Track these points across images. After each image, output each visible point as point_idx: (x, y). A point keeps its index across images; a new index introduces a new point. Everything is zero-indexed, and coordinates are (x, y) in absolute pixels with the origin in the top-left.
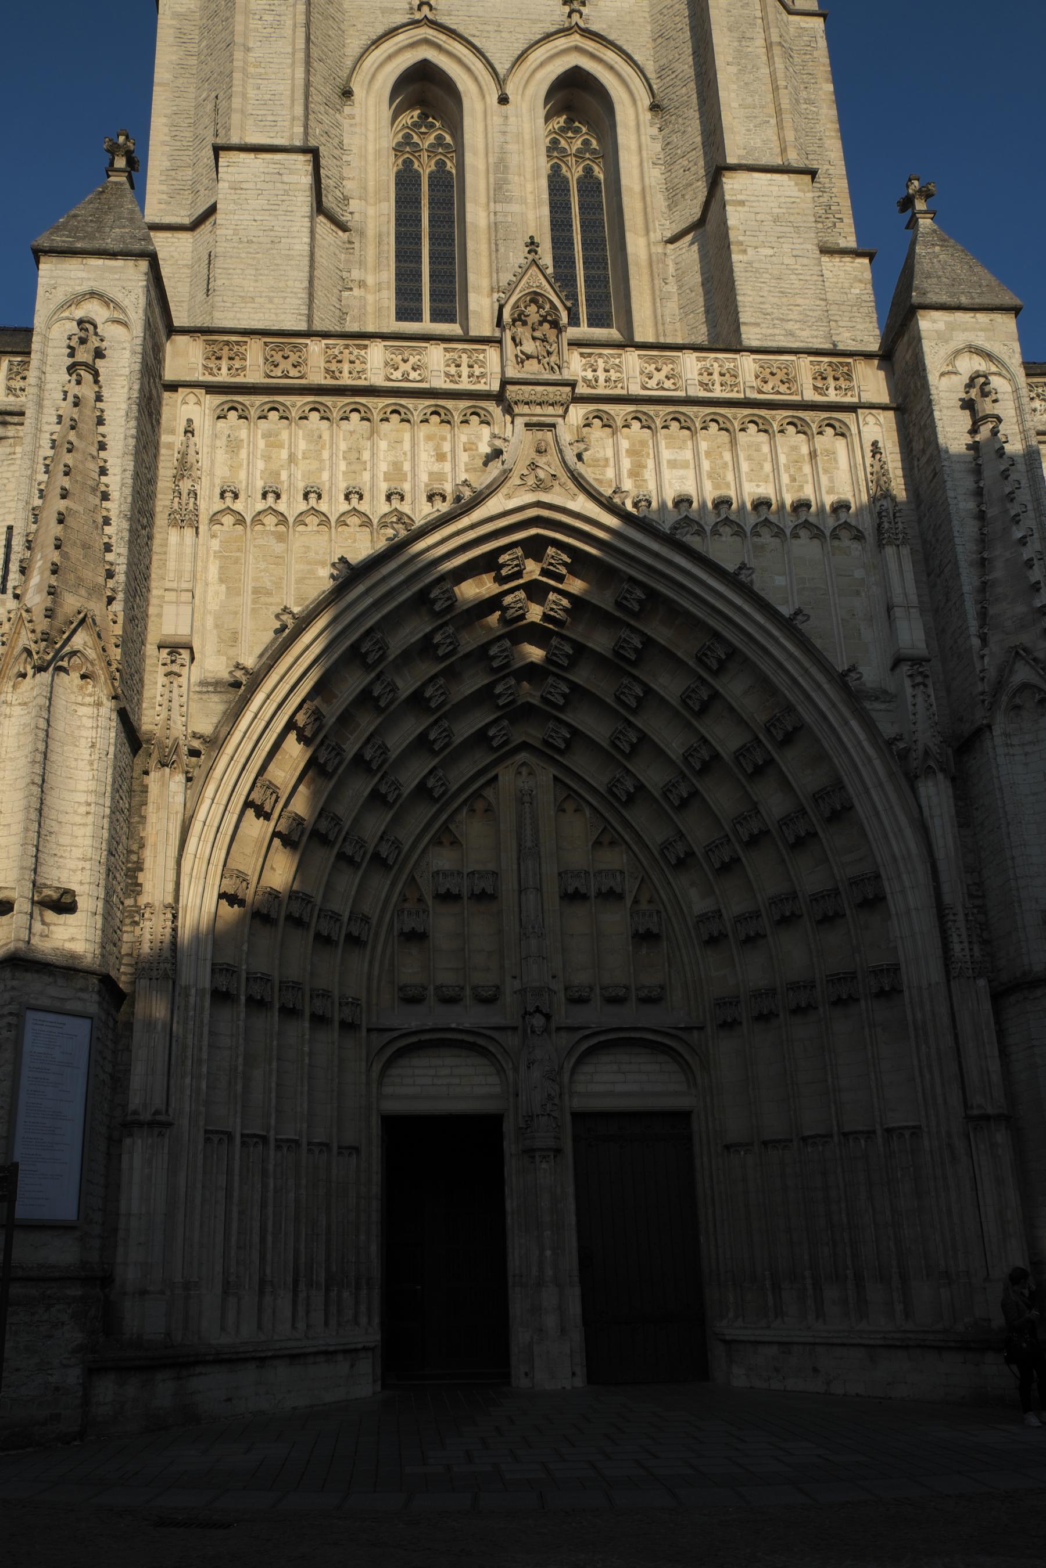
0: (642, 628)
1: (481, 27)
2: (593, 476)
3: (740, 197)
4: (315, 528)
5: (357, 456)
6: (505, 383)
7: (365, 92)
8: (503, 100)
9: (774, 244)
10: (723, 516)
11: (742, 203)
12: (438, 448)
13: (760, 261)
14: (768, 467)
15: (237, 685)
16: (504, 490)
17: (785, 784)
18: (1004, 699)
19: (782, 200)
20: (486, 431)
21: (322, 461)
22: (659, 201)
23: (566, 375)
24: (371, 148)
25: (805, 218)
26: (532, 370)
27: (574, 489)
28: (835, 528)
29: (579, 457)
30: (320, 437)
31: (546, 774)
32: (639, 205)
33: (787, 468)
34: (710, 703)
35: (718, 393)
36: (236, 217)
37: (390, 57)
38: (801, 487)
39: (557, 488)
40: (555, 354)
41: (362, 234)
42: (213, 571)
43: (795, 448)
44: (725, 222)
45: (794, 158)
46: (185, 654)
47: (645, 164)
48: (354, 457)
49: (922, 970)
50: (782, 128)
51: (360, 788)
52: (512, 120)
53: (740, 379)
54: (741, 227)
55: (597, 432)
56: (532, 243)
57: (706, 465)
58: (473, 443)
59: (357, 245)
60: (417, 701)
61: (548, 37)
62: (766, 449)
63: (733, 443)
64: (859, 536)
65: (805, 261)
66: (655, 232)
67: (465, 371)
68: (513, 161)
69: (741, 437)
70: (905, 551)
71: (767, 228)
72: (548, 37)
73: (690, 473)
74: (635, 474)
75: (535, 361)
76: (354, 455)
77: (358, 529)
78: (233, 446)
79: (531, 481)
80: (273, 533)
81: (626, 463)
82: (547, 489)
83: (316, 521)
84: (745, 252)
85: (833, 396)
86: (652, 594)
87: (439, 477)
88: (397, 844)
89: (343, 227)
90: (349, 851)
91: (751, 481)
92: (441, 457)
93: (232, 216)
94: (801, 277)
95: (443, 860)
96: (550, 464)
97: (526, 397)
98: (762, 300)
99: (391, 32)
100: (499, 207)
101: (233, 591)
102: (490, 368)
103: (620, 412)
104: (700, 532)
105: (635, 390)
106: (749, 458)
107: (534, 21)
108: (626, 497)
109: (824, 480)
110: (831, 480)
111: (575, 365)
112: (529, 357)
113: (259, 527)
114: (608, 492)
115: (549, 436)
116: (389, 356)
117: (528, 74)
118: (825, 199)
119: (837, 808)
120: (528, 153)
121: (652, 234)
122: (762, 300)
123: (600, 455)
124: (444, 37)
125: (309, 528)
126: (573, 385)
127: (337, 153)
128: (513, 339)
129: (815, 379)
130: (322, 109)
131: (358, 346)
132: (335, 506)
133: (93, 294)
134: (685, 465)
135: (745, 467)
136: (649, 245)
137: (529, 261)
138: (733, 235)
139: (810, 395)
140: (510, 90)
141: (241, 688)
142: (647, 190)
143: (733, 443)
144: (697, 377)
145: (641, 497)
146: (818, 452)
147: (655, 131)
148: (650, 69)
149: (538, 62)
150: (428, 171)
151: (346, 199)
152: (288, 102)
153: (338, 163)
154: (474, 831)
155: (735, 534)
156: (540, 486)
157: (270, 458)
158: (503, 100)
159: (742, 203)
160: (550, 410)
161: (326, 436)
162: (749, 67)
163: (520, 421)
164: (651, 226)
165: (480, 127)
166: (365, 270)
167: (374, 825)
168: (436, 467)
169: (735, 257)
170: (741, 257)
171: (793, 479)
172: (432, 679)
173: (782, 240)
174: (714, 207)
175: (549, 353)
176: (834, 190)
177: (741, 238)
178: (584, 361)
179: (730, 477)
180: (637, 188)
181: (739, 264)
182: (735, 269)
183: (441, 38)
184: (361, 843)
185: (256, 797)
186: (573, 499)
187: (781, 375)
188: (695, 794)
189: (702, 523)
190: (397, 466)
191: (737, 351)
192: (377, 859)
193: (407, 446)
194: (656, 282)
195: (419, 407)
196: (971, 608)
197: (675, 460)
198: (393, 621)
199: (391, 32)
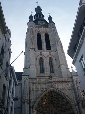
17: (68, 106)
31: (52, 105)
34: (63, 101)
72: (49, 55)
74: (57, 86)
85: (68, 81)
95: (46, 112)
99: (39, 55)
119: (71, 108)
133: (26, 78)
140: (47, 59)
141: (35, 102)
188: (62, 107)
199: (39, 55)
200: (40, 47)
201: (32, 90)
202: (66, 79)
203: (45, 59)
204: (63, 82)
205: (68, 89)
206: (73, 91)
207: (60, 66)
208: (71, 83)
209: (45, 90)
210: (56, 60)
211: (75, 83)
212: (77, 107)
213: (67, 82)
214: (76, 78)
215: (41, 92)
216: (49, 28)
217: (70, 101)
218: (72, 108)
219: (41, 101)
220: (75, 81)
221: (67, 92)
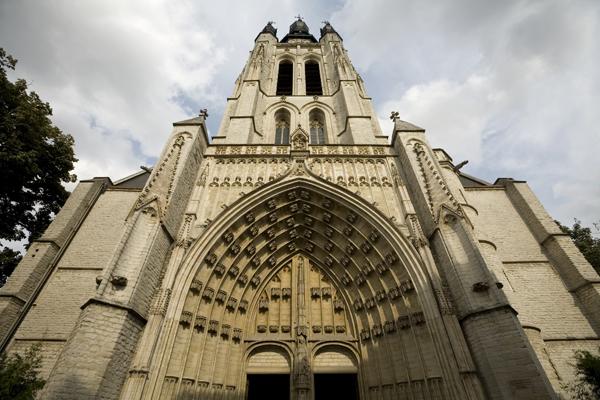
6: (291, 151)
15: (205, 226)
18: (441, 220)
42: (208, 197)
46: (193, 217)
49: (431, 313)
51: (245, 261)
60: (265, 235)
64: (391, 186)
70: (404, 187)
78: (219, 169)
86: (333, 201)
88: (259, 279)
90: (242, 279)
95: (274, 285)
101: (212, 202)
103: (322, 159)
104: (345, 185)
105: (326, 153)
139: (373, 154)
154: (284, 276)
156: (300, 174)
167: (251, 273)
172: (269, 228)
184: (246, 277)
185: (209, 258)
190: (262, 172)
192: (252, 283)
195: (268, 160)
196: (426, 197)
198: (257, 210)
201: (209, 180)
204: (354, 160)
205: (379, 185)
206: (403, 191)
207: (347, 121)
208: (391, 161)
209: (266, 181)
211: (412, 156)
212: (426, 253)
214: (414, 140)
215: (248, 190)
216: (320, 47)
217: (386, 226)
218: (396, 263)
219: (243, 229)
220: (409, 150)
221: (370, 194)
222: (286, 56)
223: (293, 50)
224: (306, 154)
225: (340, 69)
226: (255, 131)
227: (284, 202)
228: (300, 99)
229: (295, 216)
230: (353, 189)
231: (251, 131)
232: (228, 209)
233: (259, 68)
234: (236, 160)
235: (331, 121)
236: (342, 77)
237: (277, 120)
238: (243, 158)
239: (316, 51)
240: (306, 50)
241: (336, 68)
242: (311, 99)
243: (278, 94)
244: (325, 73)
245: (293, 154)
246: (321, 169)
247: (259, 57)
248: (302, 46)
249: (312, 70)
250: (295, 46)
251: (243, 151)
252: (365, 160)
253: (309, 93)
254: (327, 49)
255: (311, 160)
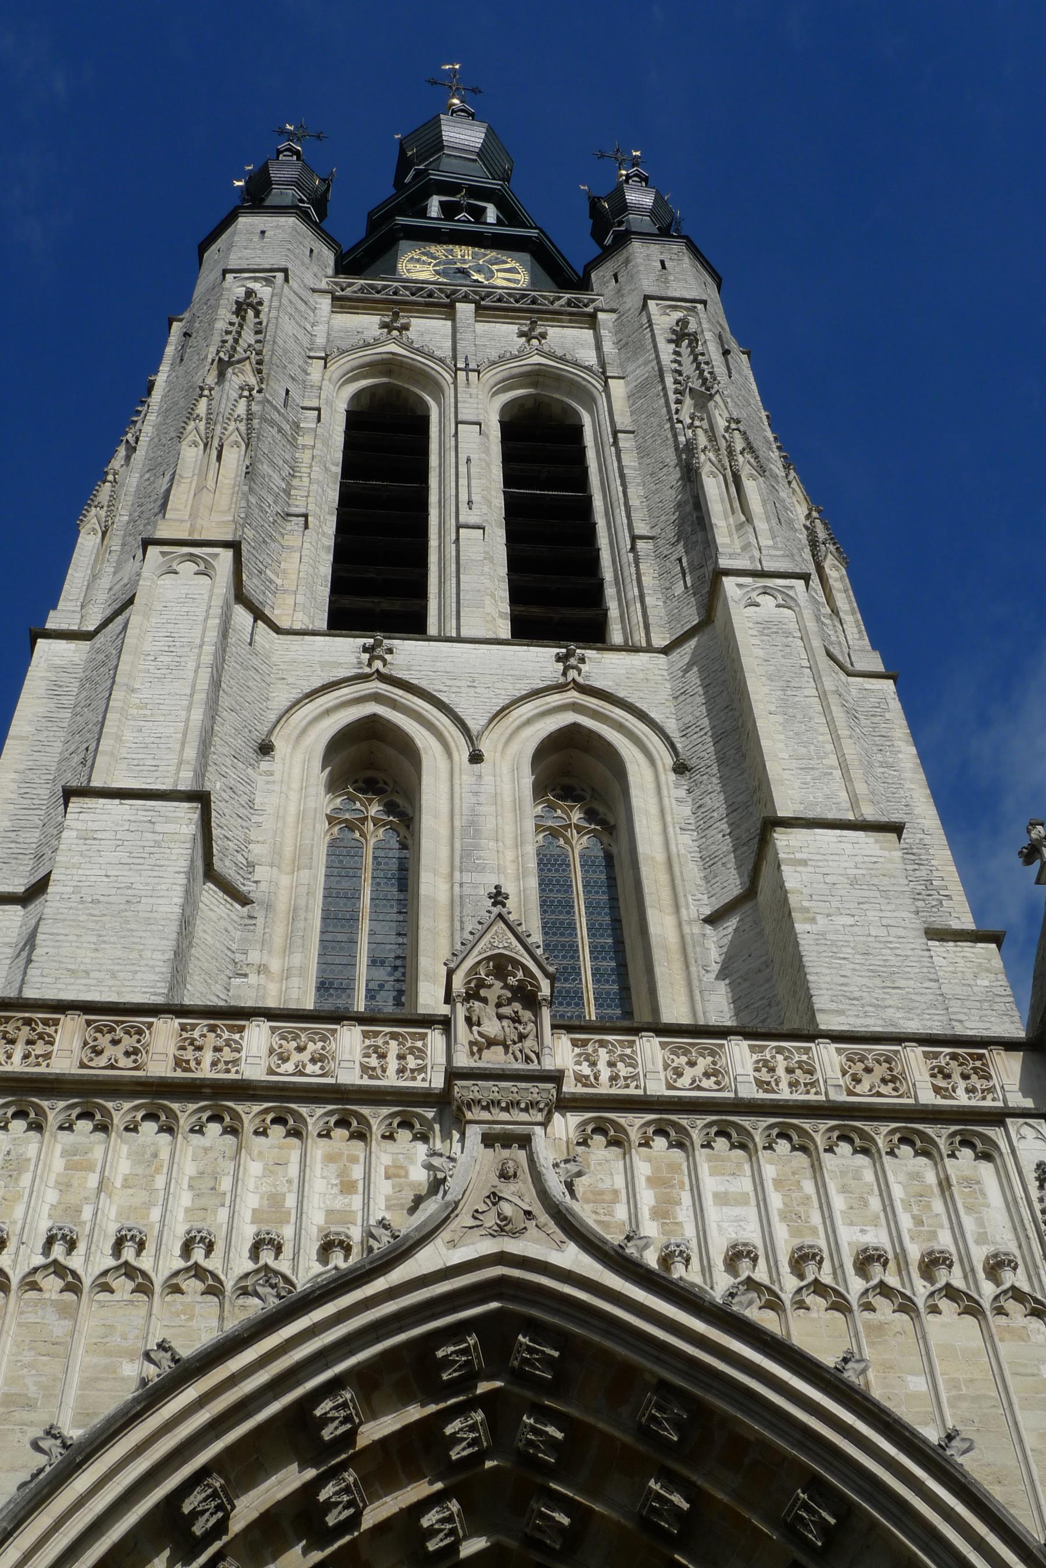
0: (685, 1472)
1: (449, 682)
2: (594, 1216)
3: (799, 856)
4: (127, 1296)
5: (211, 1184)
6: (453, 1075)
7: (291, 746)
8: (476, 758)
9: (853, 912)
10: (810, 1278)
11: (804, 863)
12: (343, 1174)
13: (836, 932)
14: (875, 1203)
16: (445, 1235)
19: (859, 859)
20: (421, 1149)
21: (153, 1191)
22: (692, 872)
23: (549, 1064)
24: (292, 809)
25: (893, 881)
26: (495, 1058)
27: (560, 1235)
28: (996, 1298)
29: (570, 1186)
30: (155, 1155)
32: (663, 878)
33: (907, 1206)
35: (785, 1094)
36: (80, 872)
37: (328, 712)
38: (933, 1235)
39: (532, 1231)
40: (532, 1036)
41: (269, 907)
43: (916, 1176)
44: (781, 885)
45: (869, 813)
47: (671, 830)
48: (206, 1186)
50: (851, 780)
52: (488, 779)
53: (818, 1075)
54: (804, 890)
55: (599, 1150)
56: (499, 893)
57: (775, 1201)
58: (401, 1167)
59: (260, 921)
61: (536, 693)
62: (869, 1176)
63: (817, 1168)
65: (901, 932)
66: (688, 908)
67: (393, 1064)
68: (488, 824)
69: (826, 1157)
71: (843, 892)
72: (536, 693)
73: (751, 1213)
74: (662, 1213)
75: (500, 1049)
76: (207, 1183)
77: (199, 1298)
79: (490, 1220)
80: (54, 1303)
81: (647, 1198)
82: (517, 1233)
83: (130, 1285)
84: (813, 920)
86: (699, 1410)
87: (345, 1216)
89: (244, 900)
91: (851, 1224)
92: (347, 1187)
93: (74, 871)
94: (898, 952)
96: (520, 1195)
97: (486, 1096)
98: (843, 980)
100: (467, 877)
102: (431, 1061)
103: (633, 1123)
104: (774, 1304)
105: (657, 1088)
106: (844, 1189)
107: (519, 678)
108: (646, 1247)
109: (969, 1223)
110: (980, 1223)
111: (561, 1053)
112: (491, 1043)
113: (33, 1294)
114: (614, 1238)
115: (522, 1155)
116: (276, 1040)
117: (509, 731)
118: (923, 873)
120: (509, 816)
121: (684, 912)
122: (843, 980)
123: (606, 1185)
124: (400, 692)
125: (116, 1296)
126: (556, 1078)
127: (242, 811)
128: (469, 1020)
129: (933, 1076)
130: (228, 762)
131: (231, 1029)
132: (162, 1262)
134: (741, 1200)
135: (838, 1202)
136: (680, 925)
137: (493, 916)
138: (793, 900)
142: (675, 859)
143: (817, 1168)
144: (751, 1073)
145: (672, 1248)
146: (954, 1180)
147: (682, 793)
148: (672, 727)
149: (524, 718)
150: (372, 841)
151: (251, 865)
152: (178, 746)
153: (244, 824)
155: (834, 1307)
156: (504, 1228)
157: (69, 1185)
158: (476, 758)
159: (804, 863)
160: (524, 1117)
161: (164, 1155)
162: (799, 716)
163: (474, 1133)
164: (682, 900)
165: (444, 788)
166: (270, 952)
168: (339, 1203)
169: (799, 927)
170: (808, 927)
171: (919, 1222)
173: (864, 906)
174: (766, 870)
175: (522, 1037)
176: (933, 862)
177: (806, 904)
178: (577, 1050)
179: (816, 1219)
180: (660, 857)
181: (806, 936)
182: (801, 942)
183: (397, 693)
186: (560, 1249)
187: (880, 1071)
189: (776, 1288)
190: (275, 1200)
191: (811, 1038)
193: (293, 1170)
194: (693, 969)
195: (314, 1116)
197: (726, 1193)
200: (380, 579)
202: (914, 1057)
203: (462, 753)
205: (972, 1308)
209: (307, 1270)
210: (681, 768)
213: (913, 1125)
222: (388, 366)
223: (429, 331)
224: (535, 1091)
225: (713, 487)
226: (210, 874)
227: (405, 1399)
228: (473, 664)
229: (464, 1483)
230: (816, 1333)
231: (190, 875)
232: (78, 1456)
233: (233, 457)
234: (121, 1111)
235: (667, 822)
236: (729, 546)
237: (333, 786)
238: (159, 1098)
239: (572, 342)
240: (505, 334)
241: (690, 475)
242: (540, 661)
243: (341, 621)
244: (625, 496)
245: (463, 1089)
246: (632, 1193)
247: (235, 379)
248: (492, 306)
249: (543, 445)
250: (440, 303)
251: (162, 1050)
252: (881, 1133)
253: (526, 629)
254: (636, 337)
255: (565, 1126)
